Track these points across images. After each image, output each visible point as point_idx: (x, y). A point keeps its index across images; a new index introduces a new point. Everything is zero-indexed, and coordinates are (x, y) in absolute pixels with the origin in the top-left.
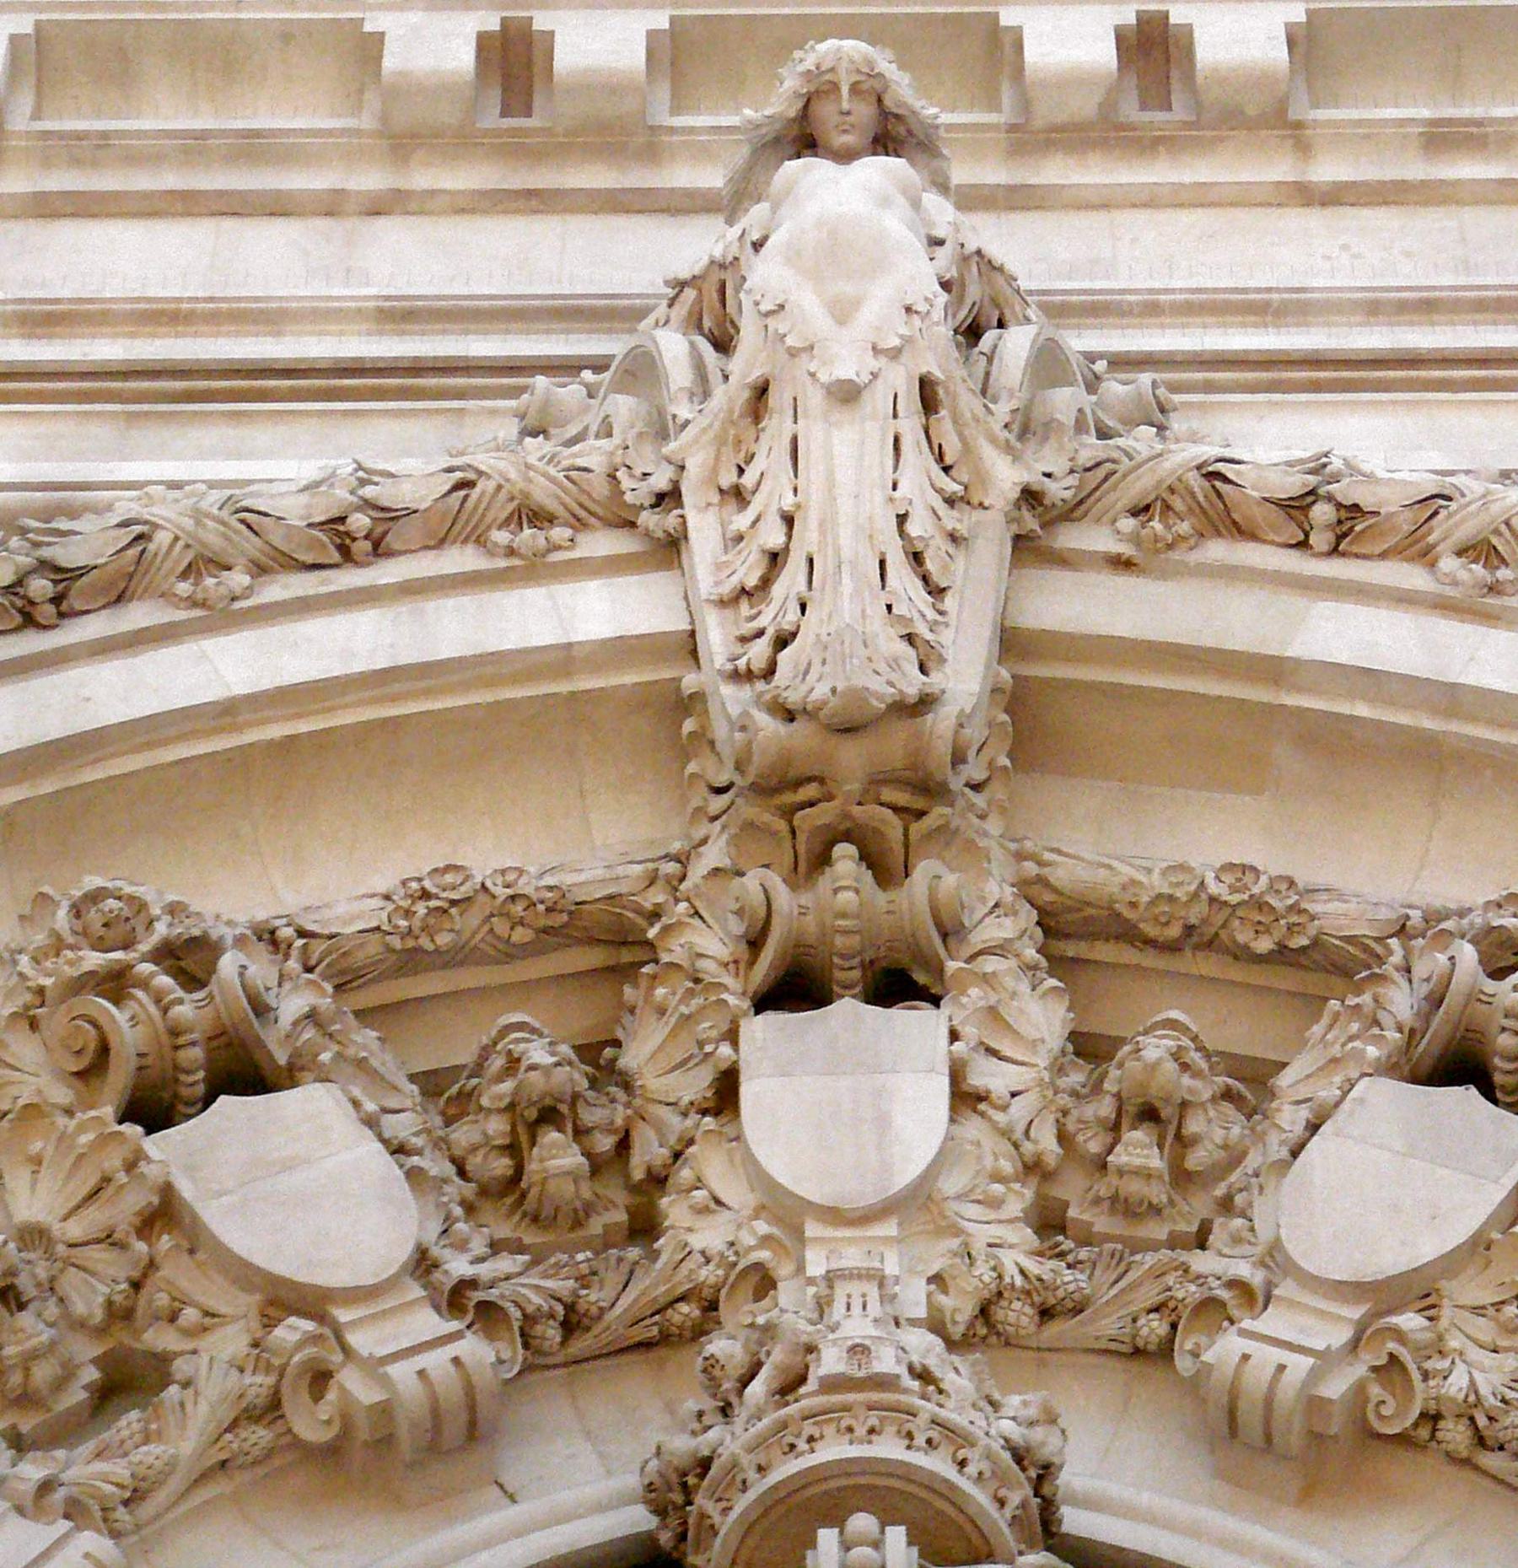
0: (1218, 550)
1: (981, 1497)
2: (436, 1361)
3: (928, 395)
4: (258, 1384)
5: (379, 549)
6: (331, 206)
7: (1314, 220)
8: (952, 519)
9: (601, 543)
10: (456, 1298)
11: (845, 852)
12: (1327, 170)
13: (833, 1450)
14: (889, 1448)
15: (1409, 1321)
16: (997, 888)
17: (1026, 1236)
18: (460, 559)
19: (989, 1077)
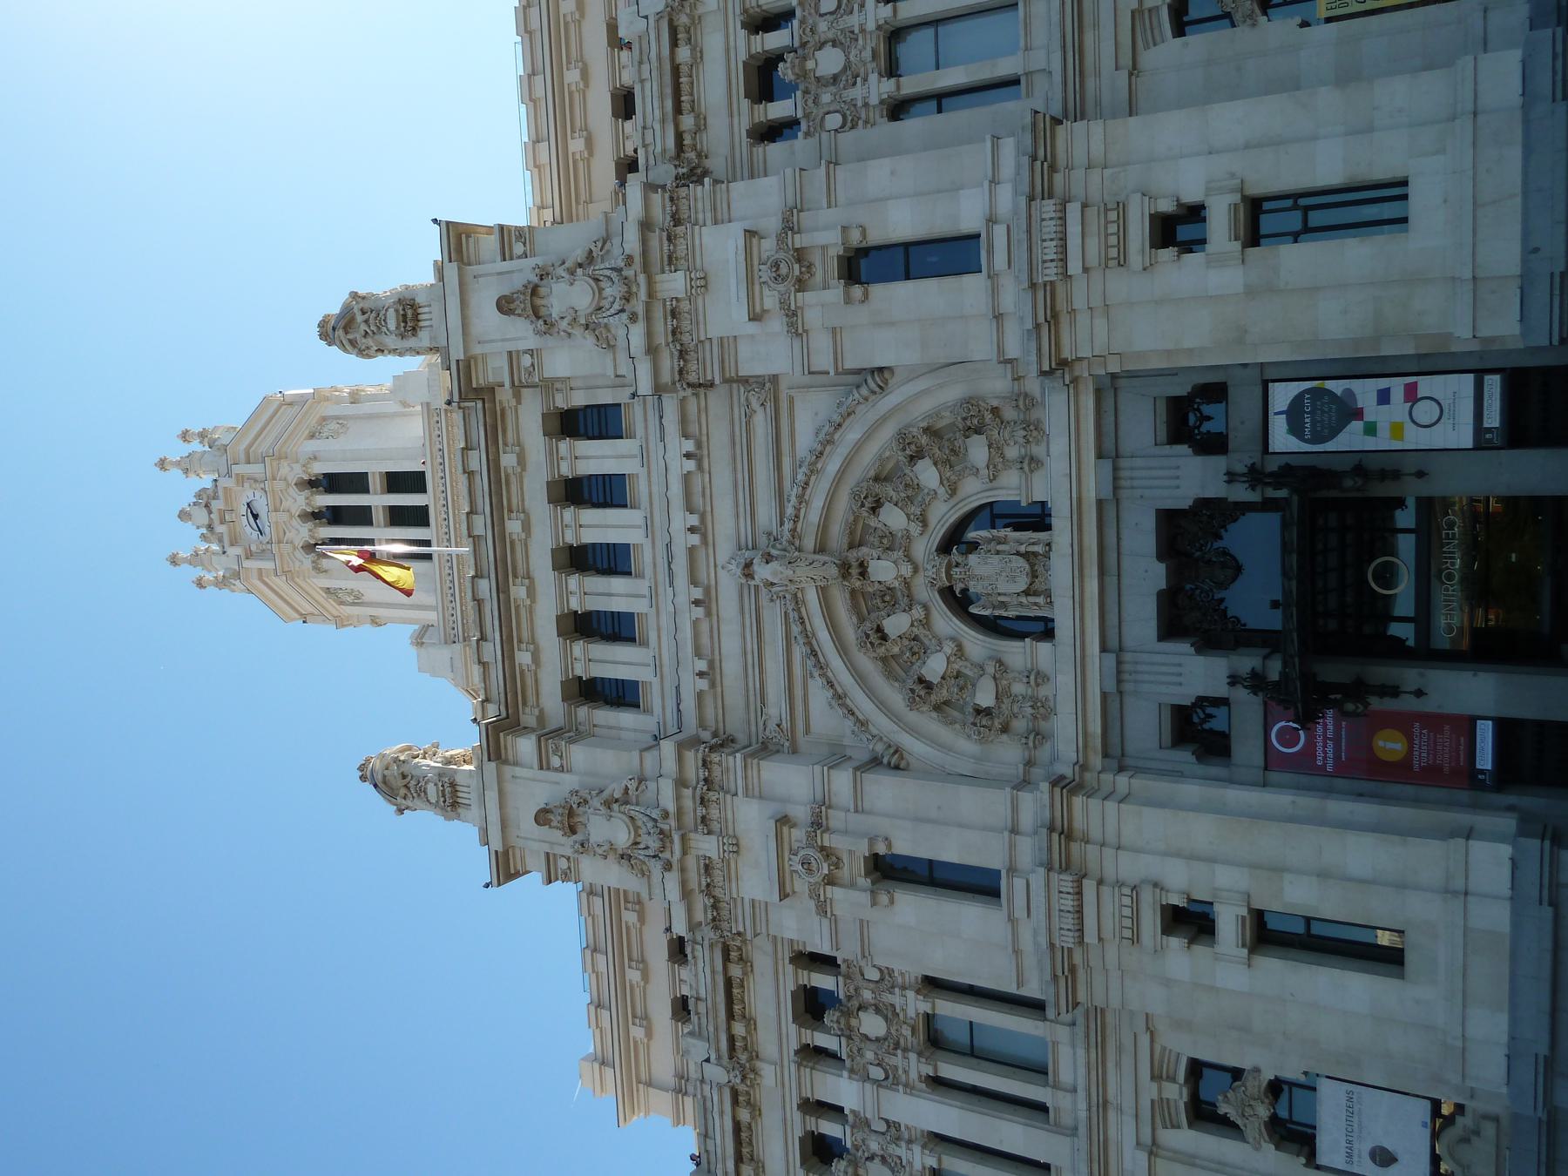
0: (799, 530)
1: (946, 561)
2: (920, 611)
3: (789, 563)
4: (921, 627)
5: (802, 618)
6: (718, 621)
7: (714, 511)
8: (804, 559)
9: (800, 595)
10: (911, 609)
11: (850, 571)
12: (709, 509)
13: (944, 575)
14: (943, 570)
15: (912, 517)
16: (848, 554)
17: (895, 553)
18: (803, 610)
19: (875, 556)
